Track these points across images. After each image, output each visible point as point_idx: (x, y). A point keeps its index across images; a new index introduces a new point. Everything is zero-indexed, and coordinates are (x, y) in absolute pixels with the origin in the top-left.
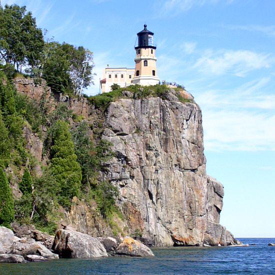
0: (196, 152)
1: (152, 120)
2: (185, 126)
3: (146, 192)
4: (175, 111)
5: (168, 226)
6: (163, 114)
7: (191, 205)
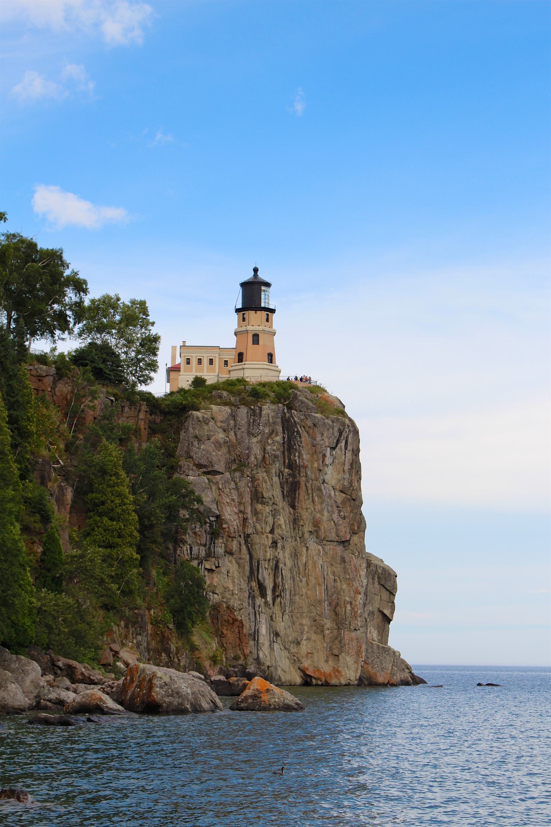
0: (349, 509)
1: (268, 448)
2: (328, 460)
3: (254, 584)
4: (311, 431)
5: (294, 650)
6: (288, 436)
7: (338, 608)
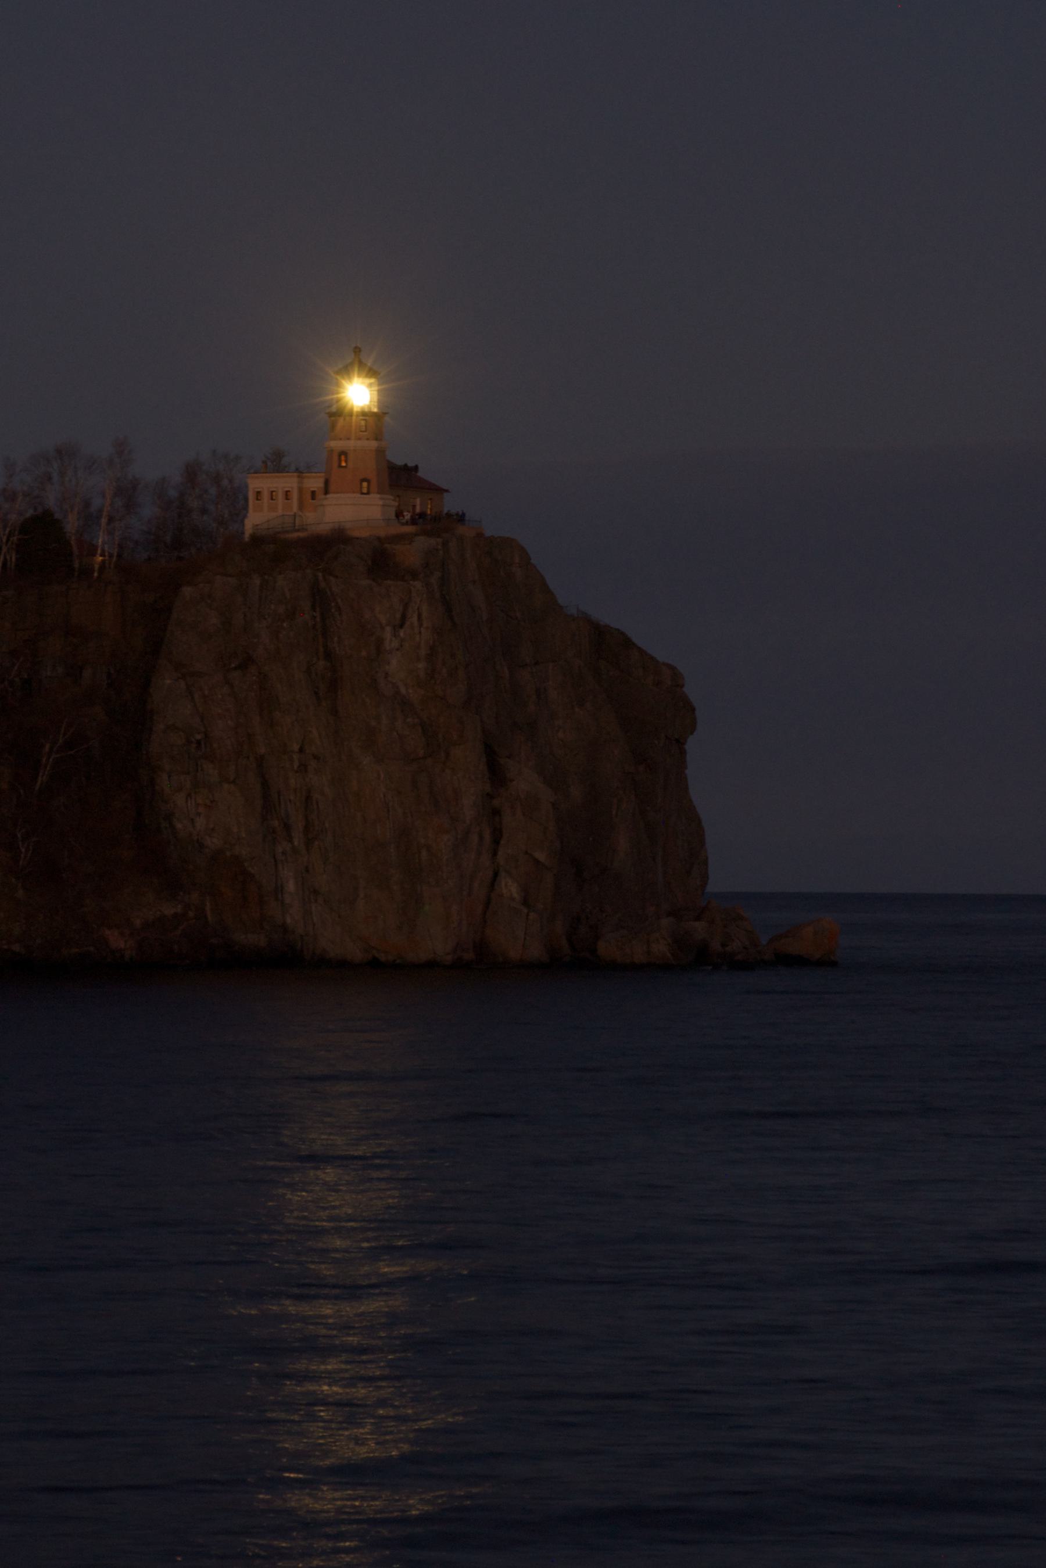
3: (276, 823)
